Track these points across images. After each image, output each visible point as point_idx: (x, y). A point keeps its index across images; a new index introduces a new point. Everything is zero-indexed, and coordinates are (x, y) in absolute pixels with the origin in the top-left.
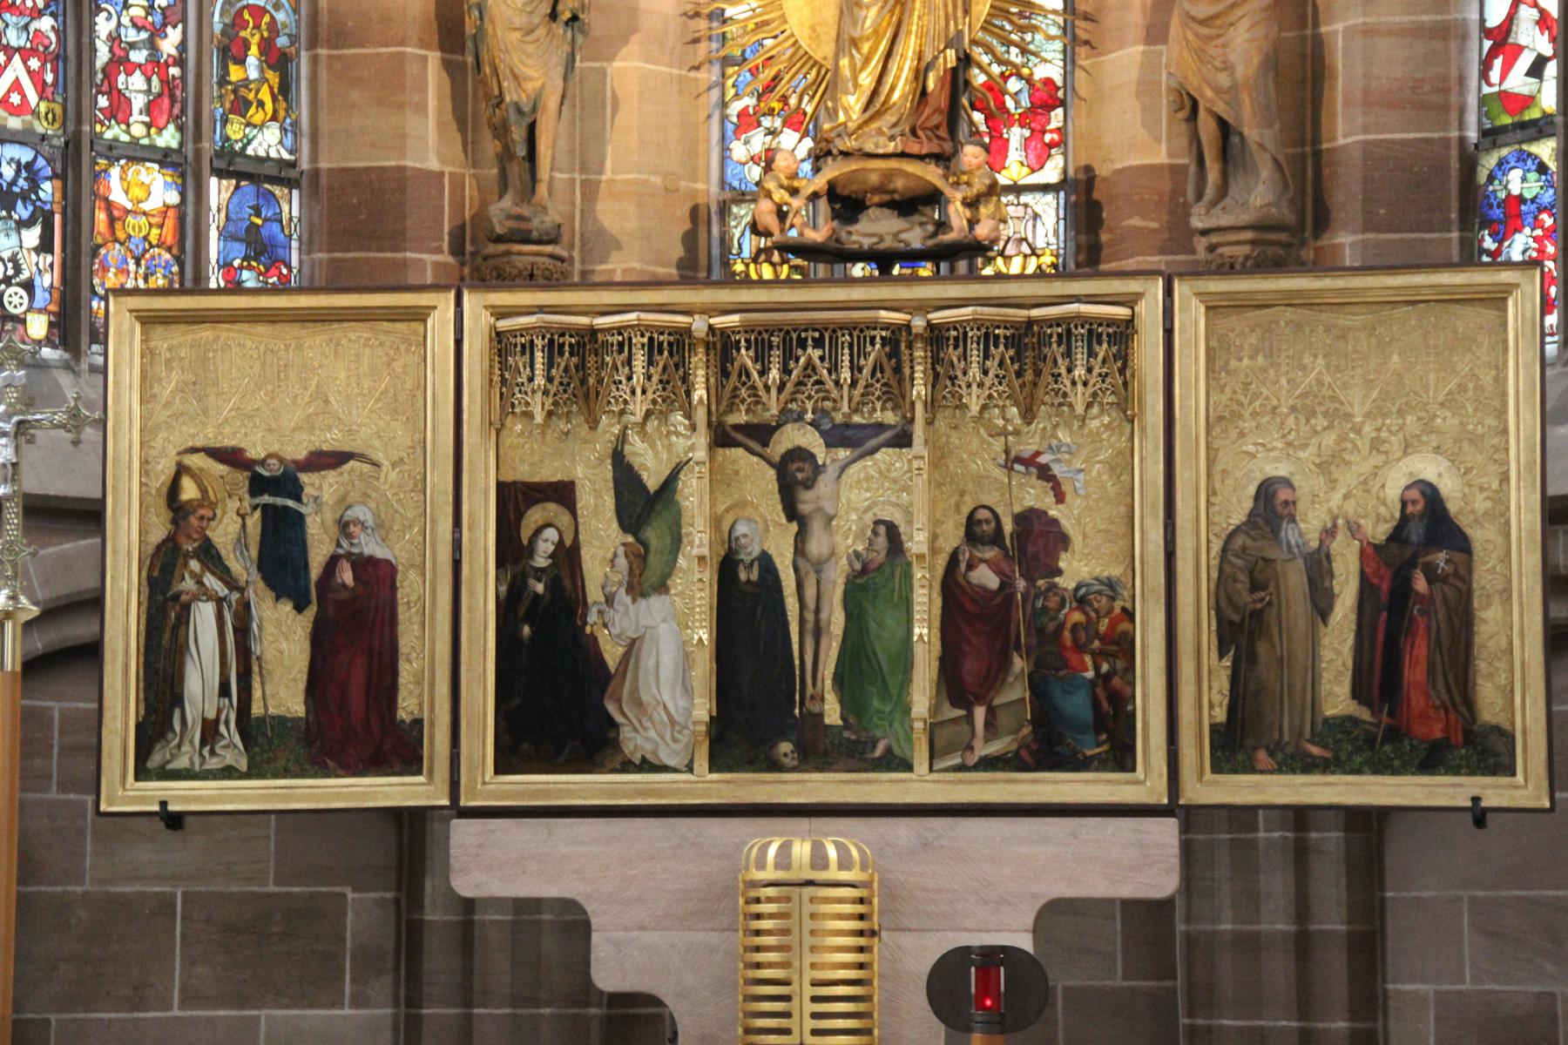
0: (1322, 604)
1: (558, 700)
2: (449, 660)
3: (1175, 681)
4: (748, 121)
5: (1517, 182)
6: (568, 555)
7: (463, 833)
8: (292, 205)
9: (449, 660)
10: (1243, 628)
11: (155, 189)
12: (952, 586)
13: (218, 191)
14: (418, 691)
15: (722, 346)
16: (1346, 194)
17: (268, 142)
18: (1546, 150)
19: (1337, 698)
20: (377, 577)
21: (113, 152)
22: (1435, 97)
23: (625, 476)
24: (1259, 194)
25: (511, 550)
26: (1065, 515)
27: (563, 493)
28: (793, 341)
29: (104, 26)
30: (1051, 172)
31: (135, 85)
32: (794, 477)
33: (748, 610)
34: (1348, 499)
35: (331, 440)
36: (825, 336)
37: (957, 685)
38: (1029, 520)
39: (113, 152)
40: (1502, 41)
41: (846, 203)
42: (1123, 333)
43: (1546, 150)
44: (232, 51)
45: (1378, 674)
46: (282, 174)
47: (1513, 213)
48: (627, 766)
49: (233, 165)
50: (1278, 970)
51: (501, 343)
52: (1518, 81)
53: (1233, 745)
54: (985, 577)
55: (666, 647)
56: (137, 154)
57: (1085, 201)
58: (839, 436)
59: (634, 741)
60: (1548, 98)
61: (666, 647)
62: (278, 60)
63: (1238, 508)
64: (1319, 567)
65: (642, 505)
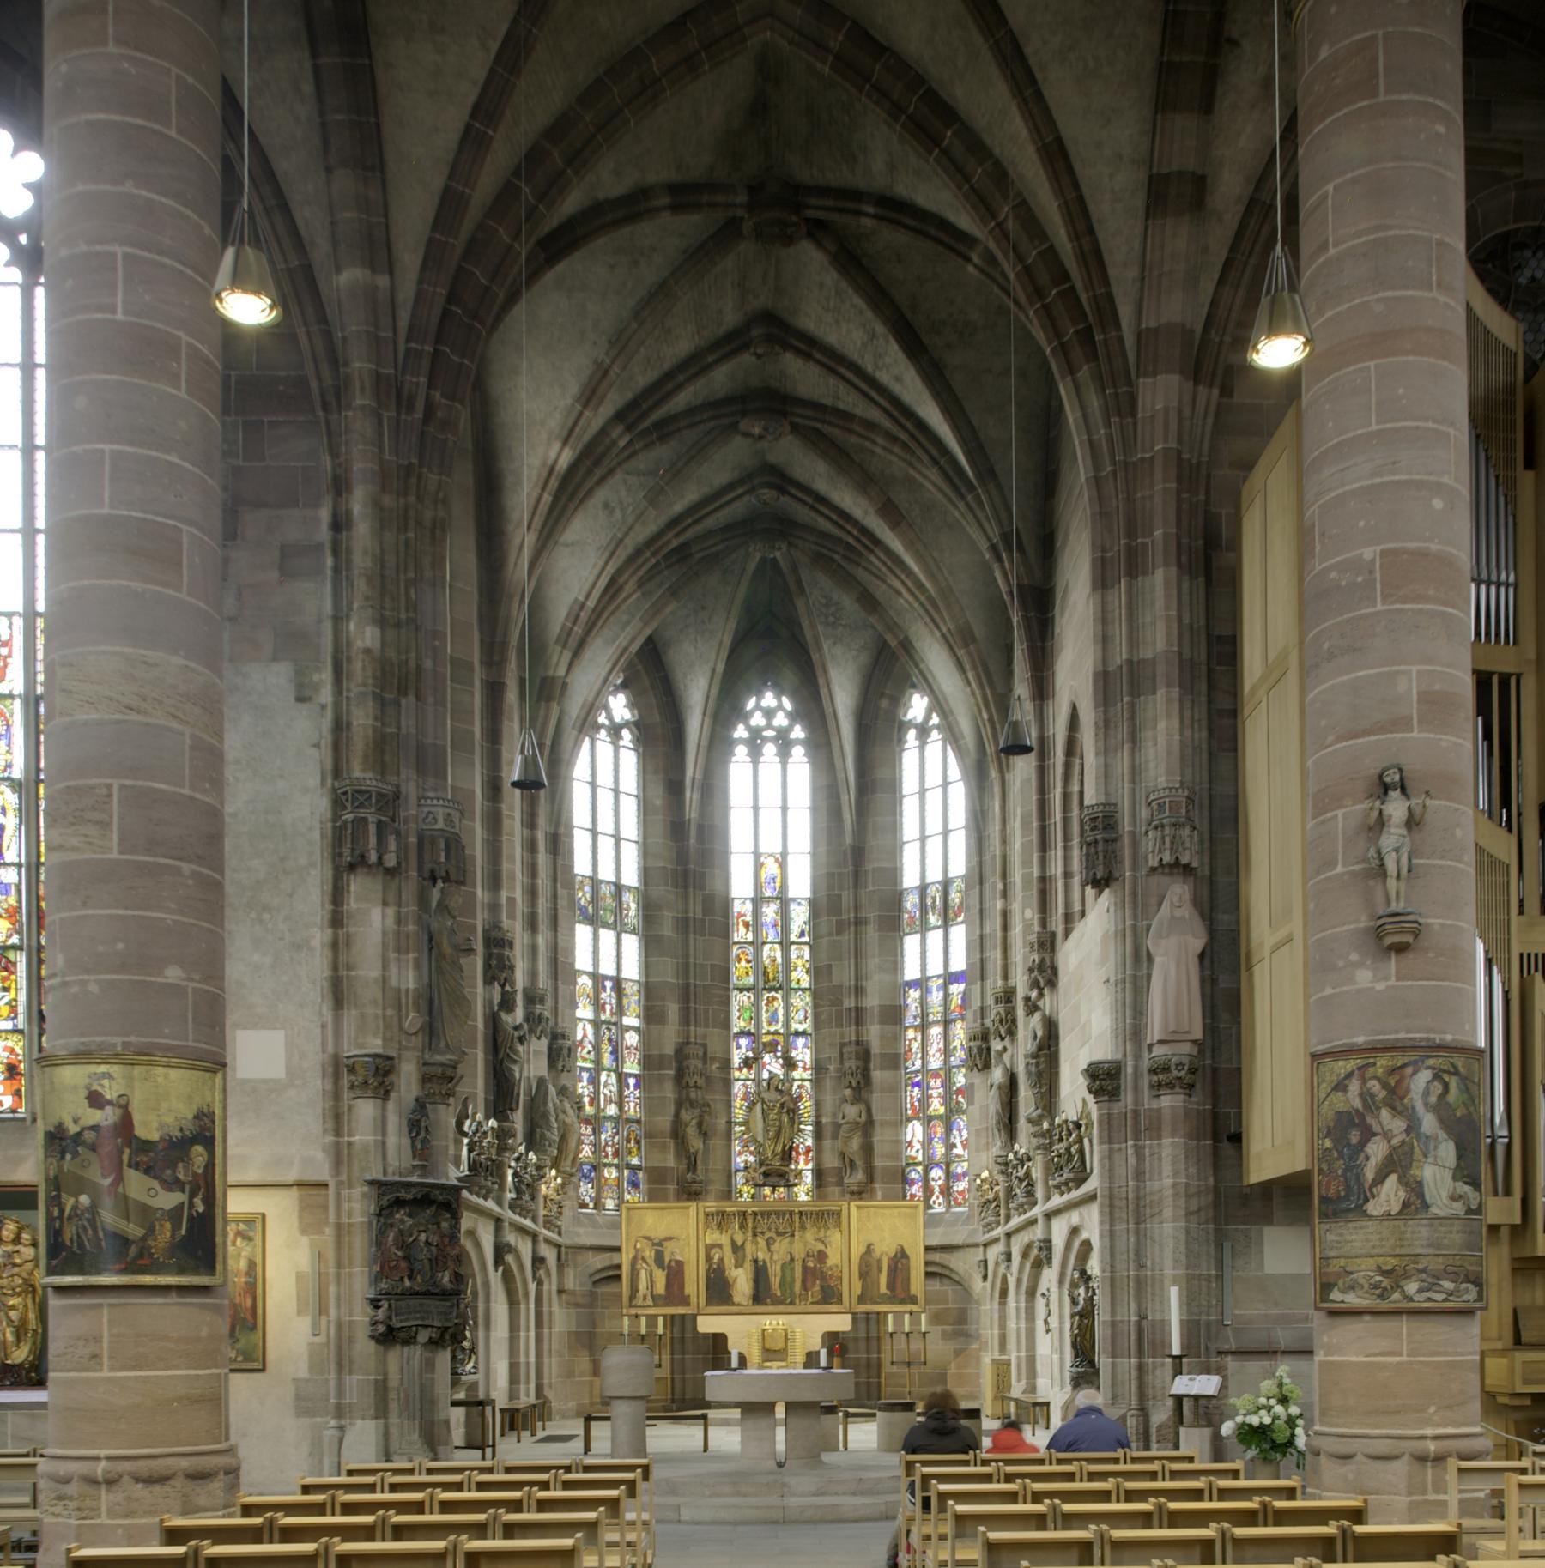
0: (880, 1270)
1: (719, 1291)
2: (695, 1284)
3: (851, 1287)
4: (740, 1154)
5: (913, 1175)
6: (721, 1260)
7: (699, 1318)
8: (641, 1175)
9: (695, 1284)
10: (864, 1275)
11: (614, 1173)
12: (805, 1268)
13: (626, 1172)
14: (690, 1289)
15: (755, 1214)
16: (878, 1175)
17: (635, 1161)
18: (920, 1169)
19: (883, 1289)
20: (680, 1264)
21: (605, 1165)
22: (896, 1155)
23: (733, 1243)
24: (860, 1175)
25: (709, 1259)
26: (829, 1251)
27: (720, 1246)
28: (770, 1214)
29: (603, 1137)
30: (810, 1166)
31: (609, 1150)
32: (769, 1243)
33: (760, 1275)
34: (885, 1248)
35: (668, 1234)
36: (777, 1213)
37: (805, 1287)
38: (820, 1252)
39: (605, 1165)
40: (910, 1143)
41: (766, 1175)
42: (839, 1214)
43: (920, 1169)
44: (628, 1141)
45: (891, 1285)
46: (639, 1168)
47: (912, 1182)
48: (733, 1304)
49: (628, 1166)
50: (862, 1345)
51: (707, 1215)
52: (913, 1153)
53: (862, 1299)
54: (811, 1264)
55: (742, 1282)
56: (610, 1165)
57: (819, 1174)
58: (778, 1234)
59: (736, 1299)
60: (920, 1158)
61: (742, 1282)
62: (638, 1142)
63: (863, 1250)
64: (879, 1261)
65: (737, 1249)
